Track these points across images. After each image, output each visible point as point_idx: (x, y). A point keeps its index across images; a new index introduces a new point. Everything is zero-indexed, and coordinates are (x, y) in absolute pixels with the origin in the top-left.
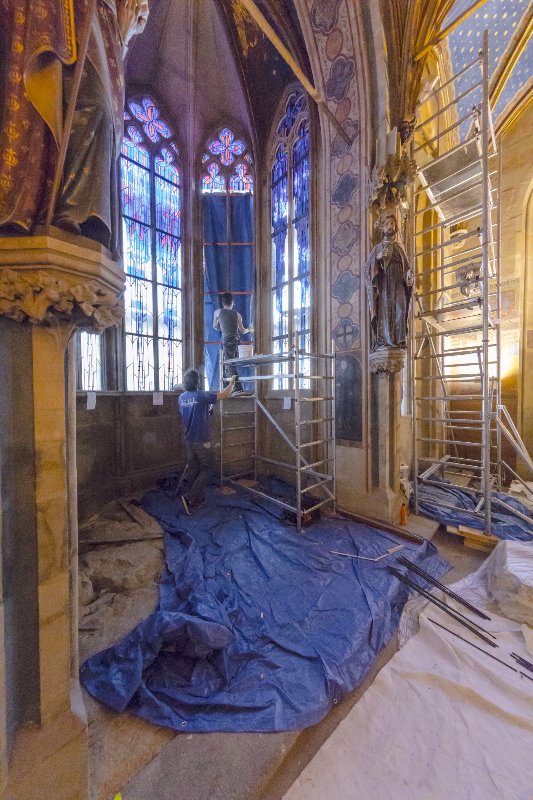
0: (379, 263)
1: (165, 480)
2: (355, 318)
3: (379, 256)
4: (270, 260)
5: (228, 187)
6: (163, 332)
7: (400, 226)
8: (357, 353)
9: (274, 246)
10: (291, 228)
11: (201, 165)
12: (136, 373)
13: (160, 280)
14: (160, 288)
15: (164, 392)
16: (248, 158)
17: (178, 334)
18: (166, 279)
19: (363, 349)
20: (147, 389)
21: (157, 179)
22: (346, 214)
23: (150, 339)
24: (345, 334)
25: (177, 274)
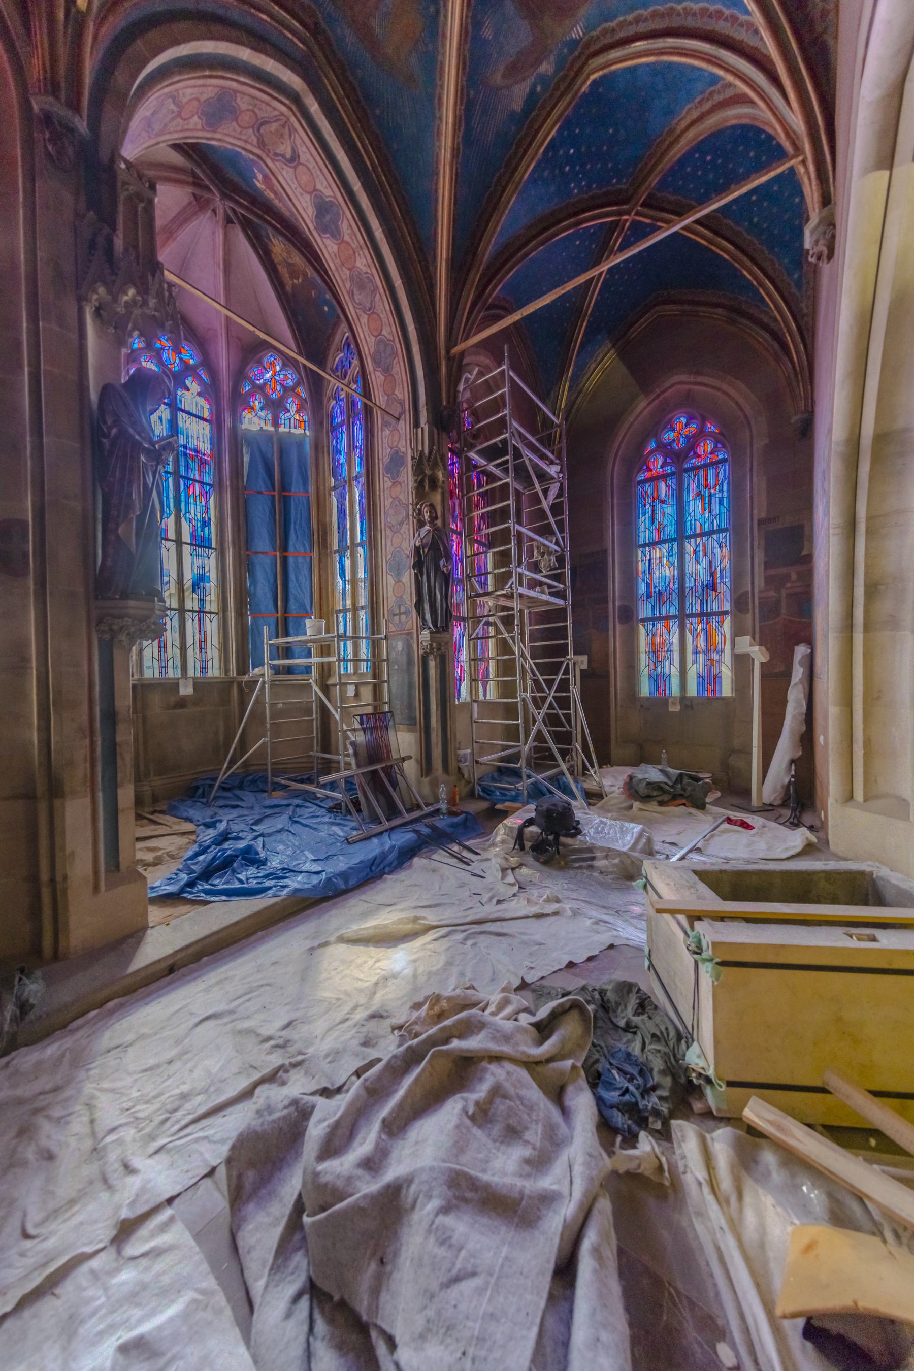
0: (417, 549)
1: (197, 788)
2: (407, 597)
3: (418, 544)
4: (331, 517)
5: (276, 423)
6: (191, 603)
7: (439, 514)
8: (409, 634)
9: (335, 500)
10: (350, 486)
11: (241, 395)
12: (156, 655)
13: (186, 538)
14: (187, 550)
15: (194, 679)
16: (302, 391)
17: (212, 604)
18: (193, 536)
19: (415, 631)
20: (171, 675)
21: (180, 415)
22: (397, 491)
23: (173, 613)
24: (400, 614)
25: (210, 529)
